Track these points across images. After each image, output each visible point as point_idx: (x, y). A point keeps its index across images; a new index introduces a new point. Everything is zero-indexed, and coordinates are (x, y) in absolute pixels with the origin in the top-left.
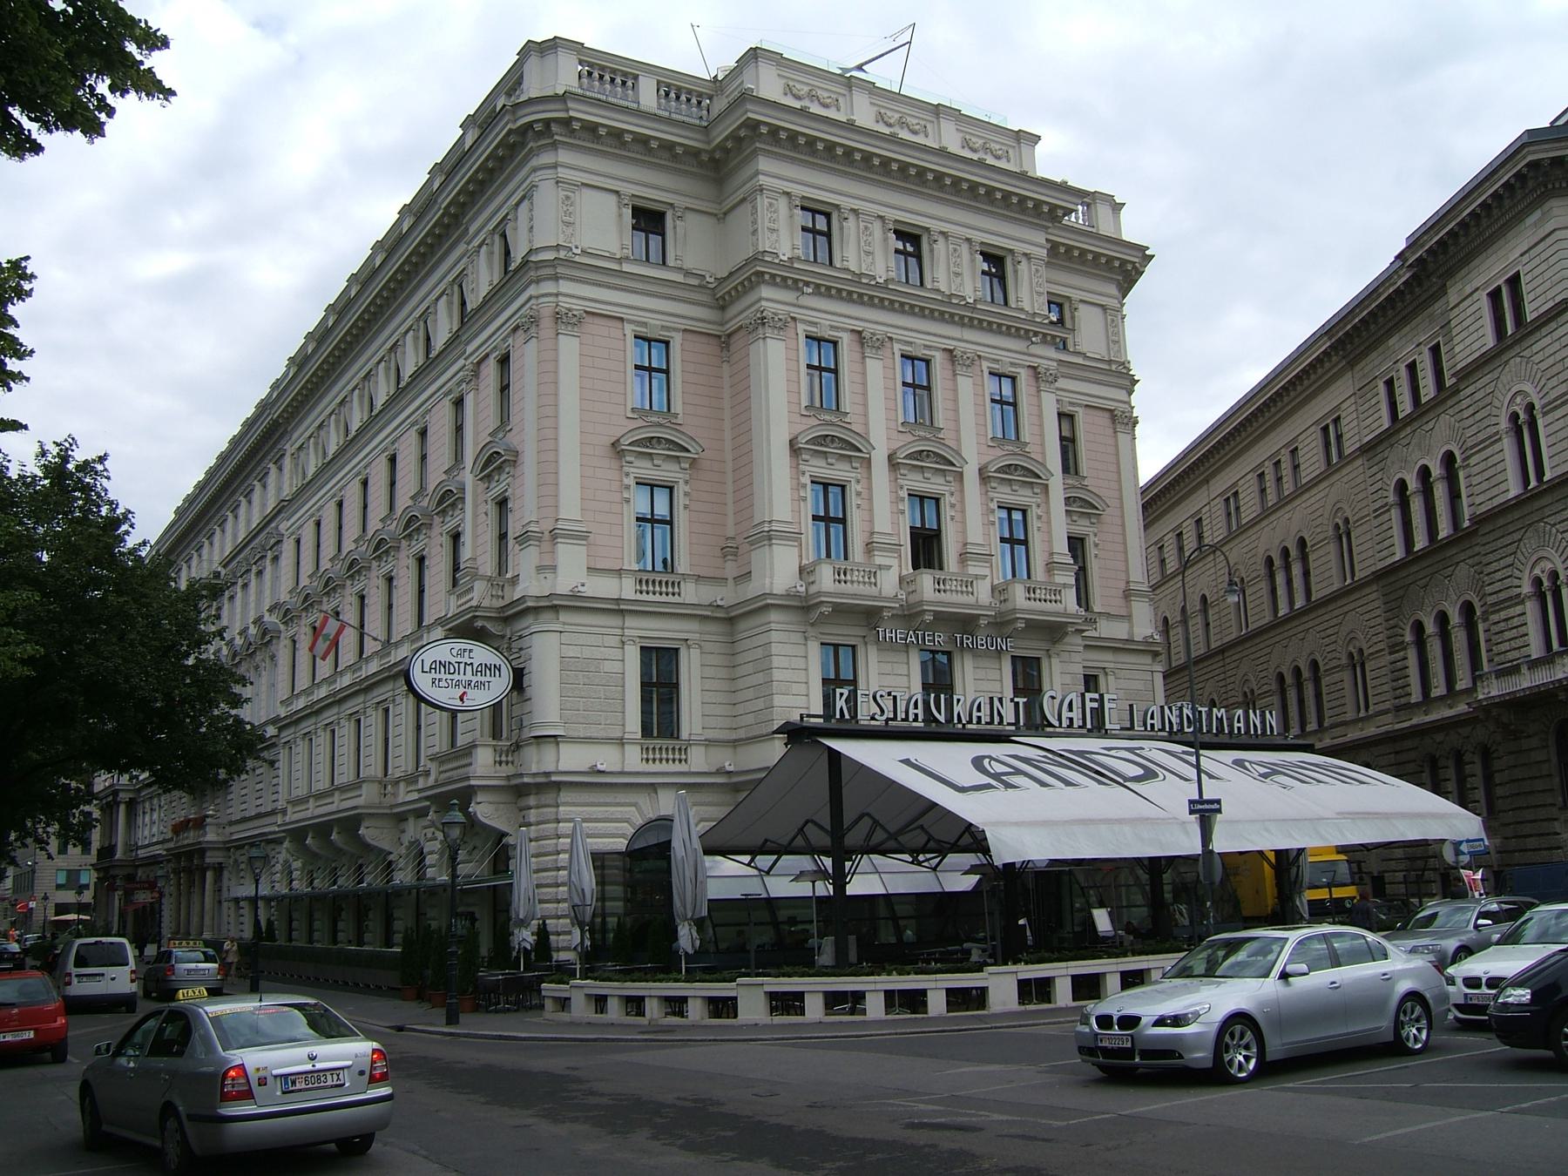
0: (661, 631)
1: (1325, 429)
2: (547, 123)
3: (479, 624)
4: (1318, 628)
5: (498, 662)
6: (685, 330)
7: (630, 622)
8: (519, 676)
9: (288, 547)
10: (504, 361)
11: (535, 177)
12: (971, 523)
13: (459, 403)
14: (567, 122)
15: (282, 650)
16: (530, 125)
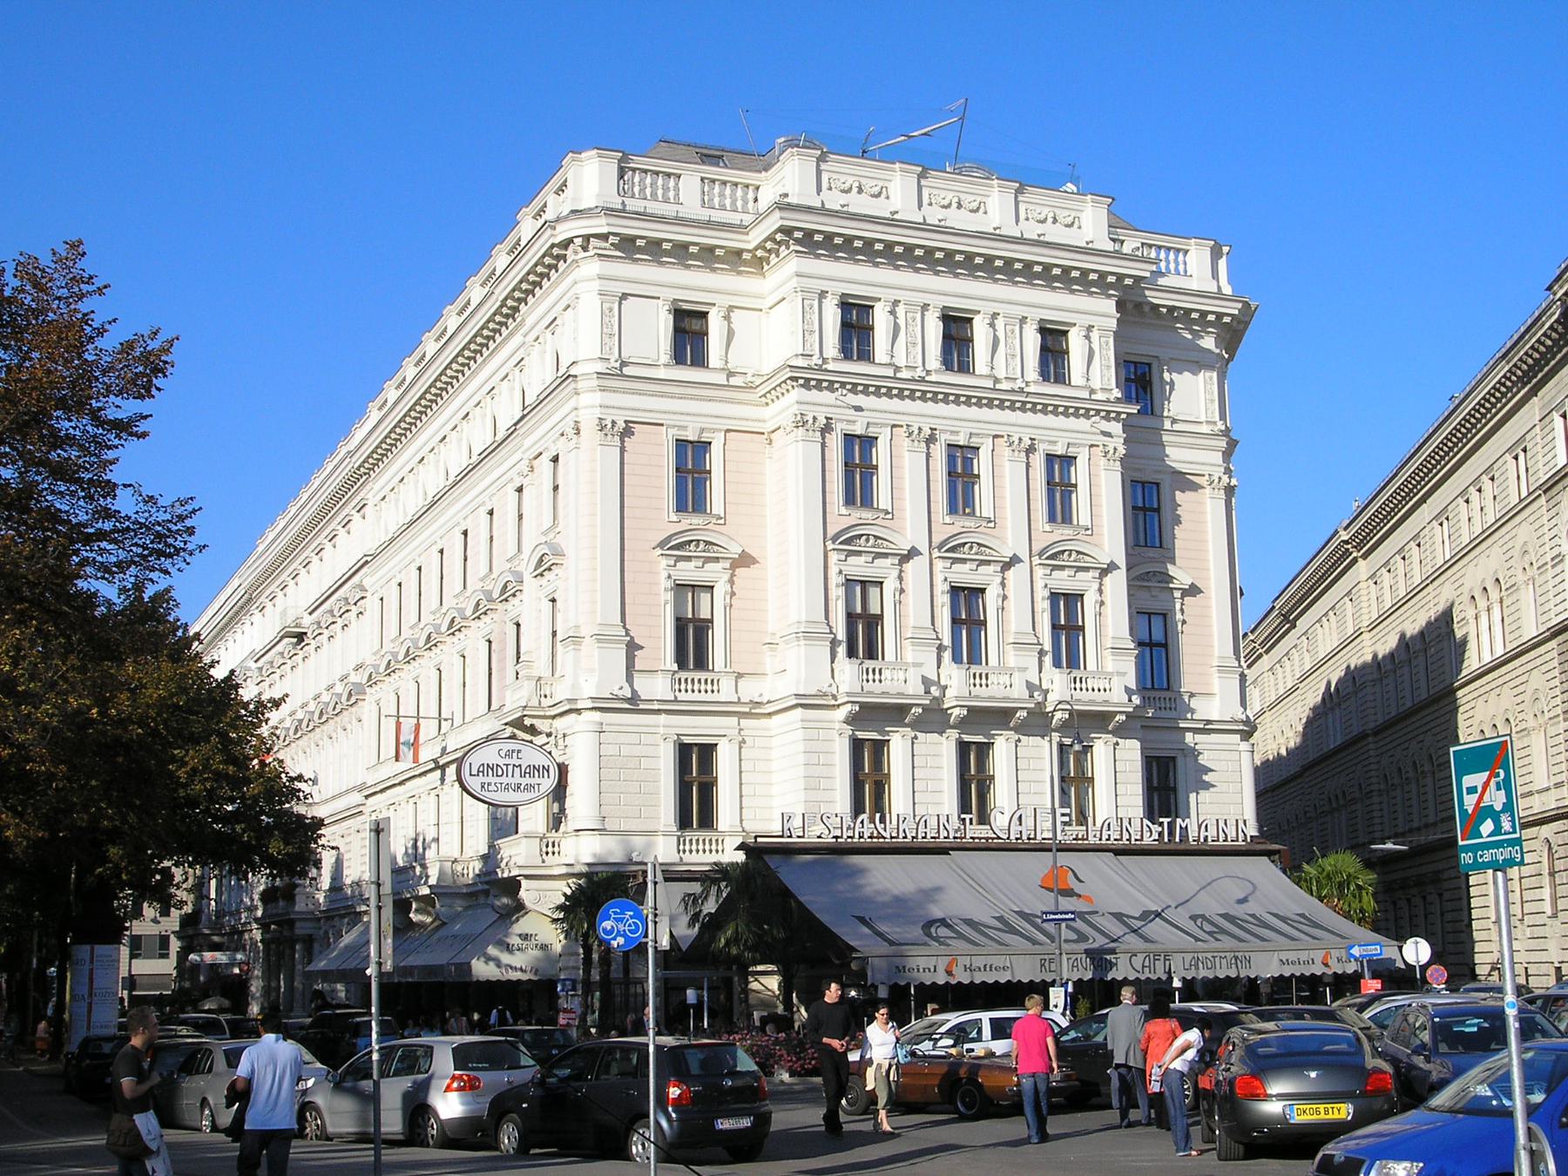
0: (697, 729)
1: (1516, 458)
2: (587, 238)
3: (527, 722)
4: (1512, 684)
5: (546, 763)
6: (728, 431)
7: (663, 718)
8: (563, 770)
9: (371, 604)
10: (555, 459)
11: (578, 288)
12: (1015, 613)
13: (520, 490)
14: (604, 237)
15: (367, 709)
16: (570, 241)
